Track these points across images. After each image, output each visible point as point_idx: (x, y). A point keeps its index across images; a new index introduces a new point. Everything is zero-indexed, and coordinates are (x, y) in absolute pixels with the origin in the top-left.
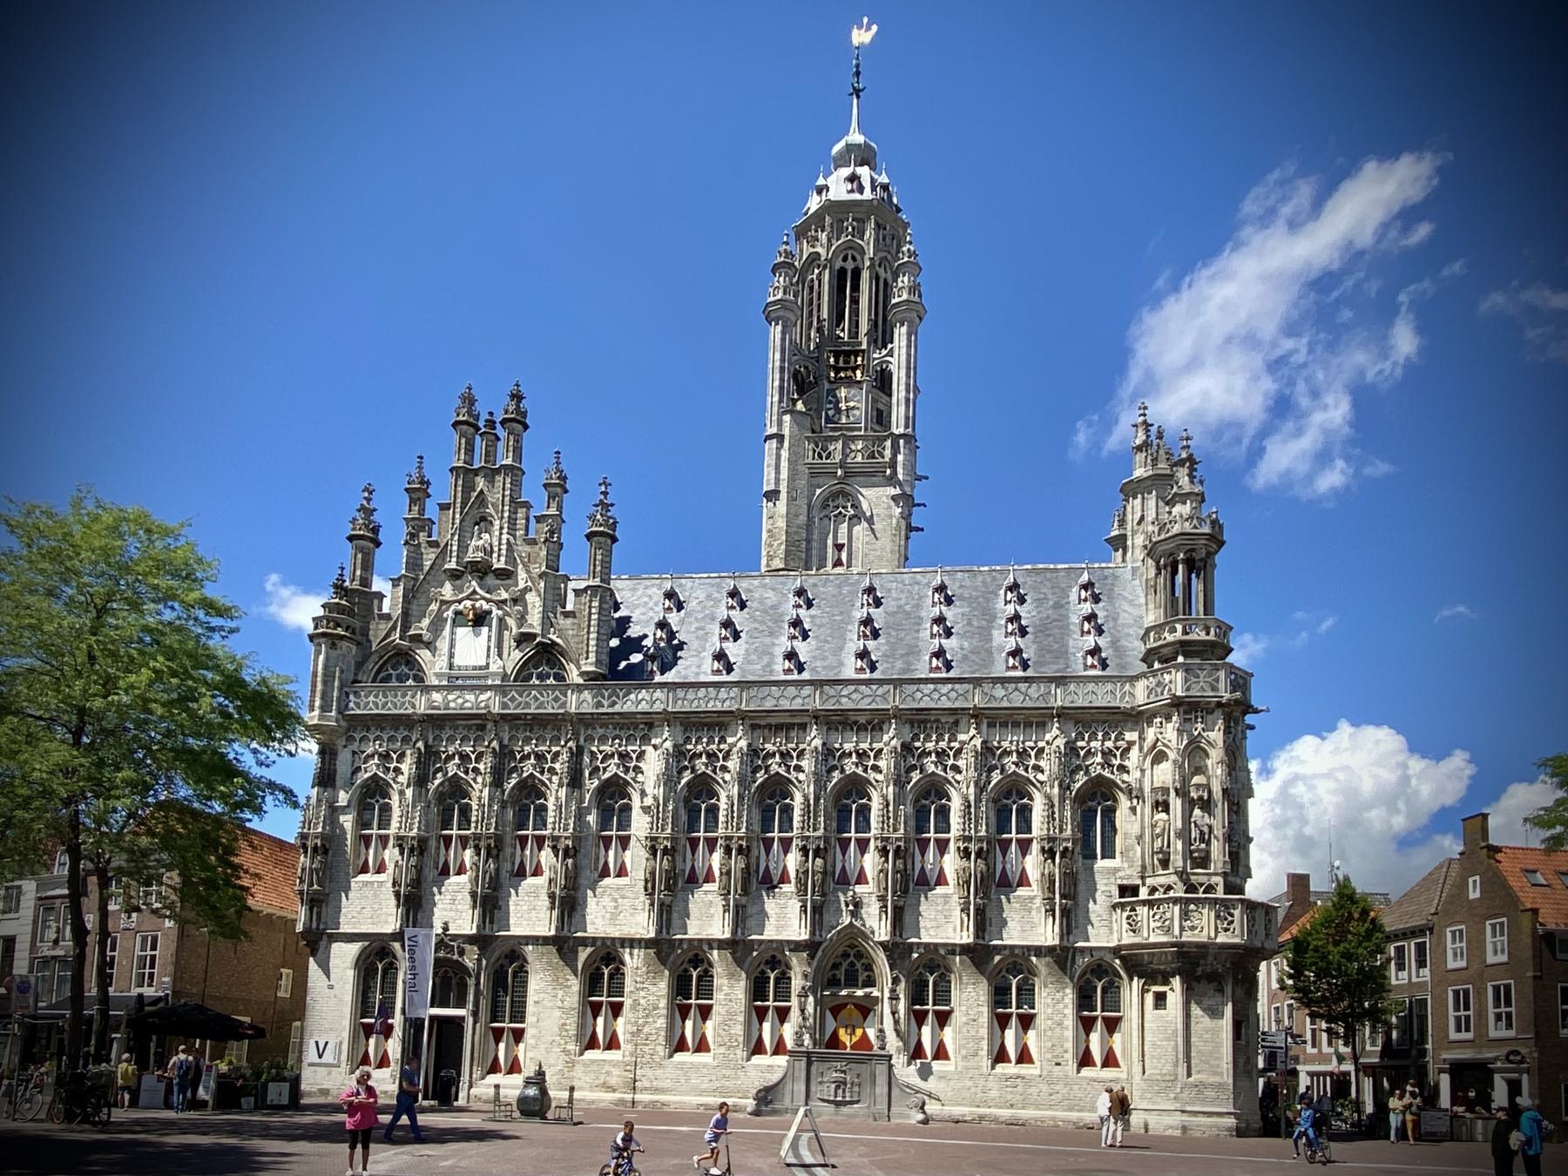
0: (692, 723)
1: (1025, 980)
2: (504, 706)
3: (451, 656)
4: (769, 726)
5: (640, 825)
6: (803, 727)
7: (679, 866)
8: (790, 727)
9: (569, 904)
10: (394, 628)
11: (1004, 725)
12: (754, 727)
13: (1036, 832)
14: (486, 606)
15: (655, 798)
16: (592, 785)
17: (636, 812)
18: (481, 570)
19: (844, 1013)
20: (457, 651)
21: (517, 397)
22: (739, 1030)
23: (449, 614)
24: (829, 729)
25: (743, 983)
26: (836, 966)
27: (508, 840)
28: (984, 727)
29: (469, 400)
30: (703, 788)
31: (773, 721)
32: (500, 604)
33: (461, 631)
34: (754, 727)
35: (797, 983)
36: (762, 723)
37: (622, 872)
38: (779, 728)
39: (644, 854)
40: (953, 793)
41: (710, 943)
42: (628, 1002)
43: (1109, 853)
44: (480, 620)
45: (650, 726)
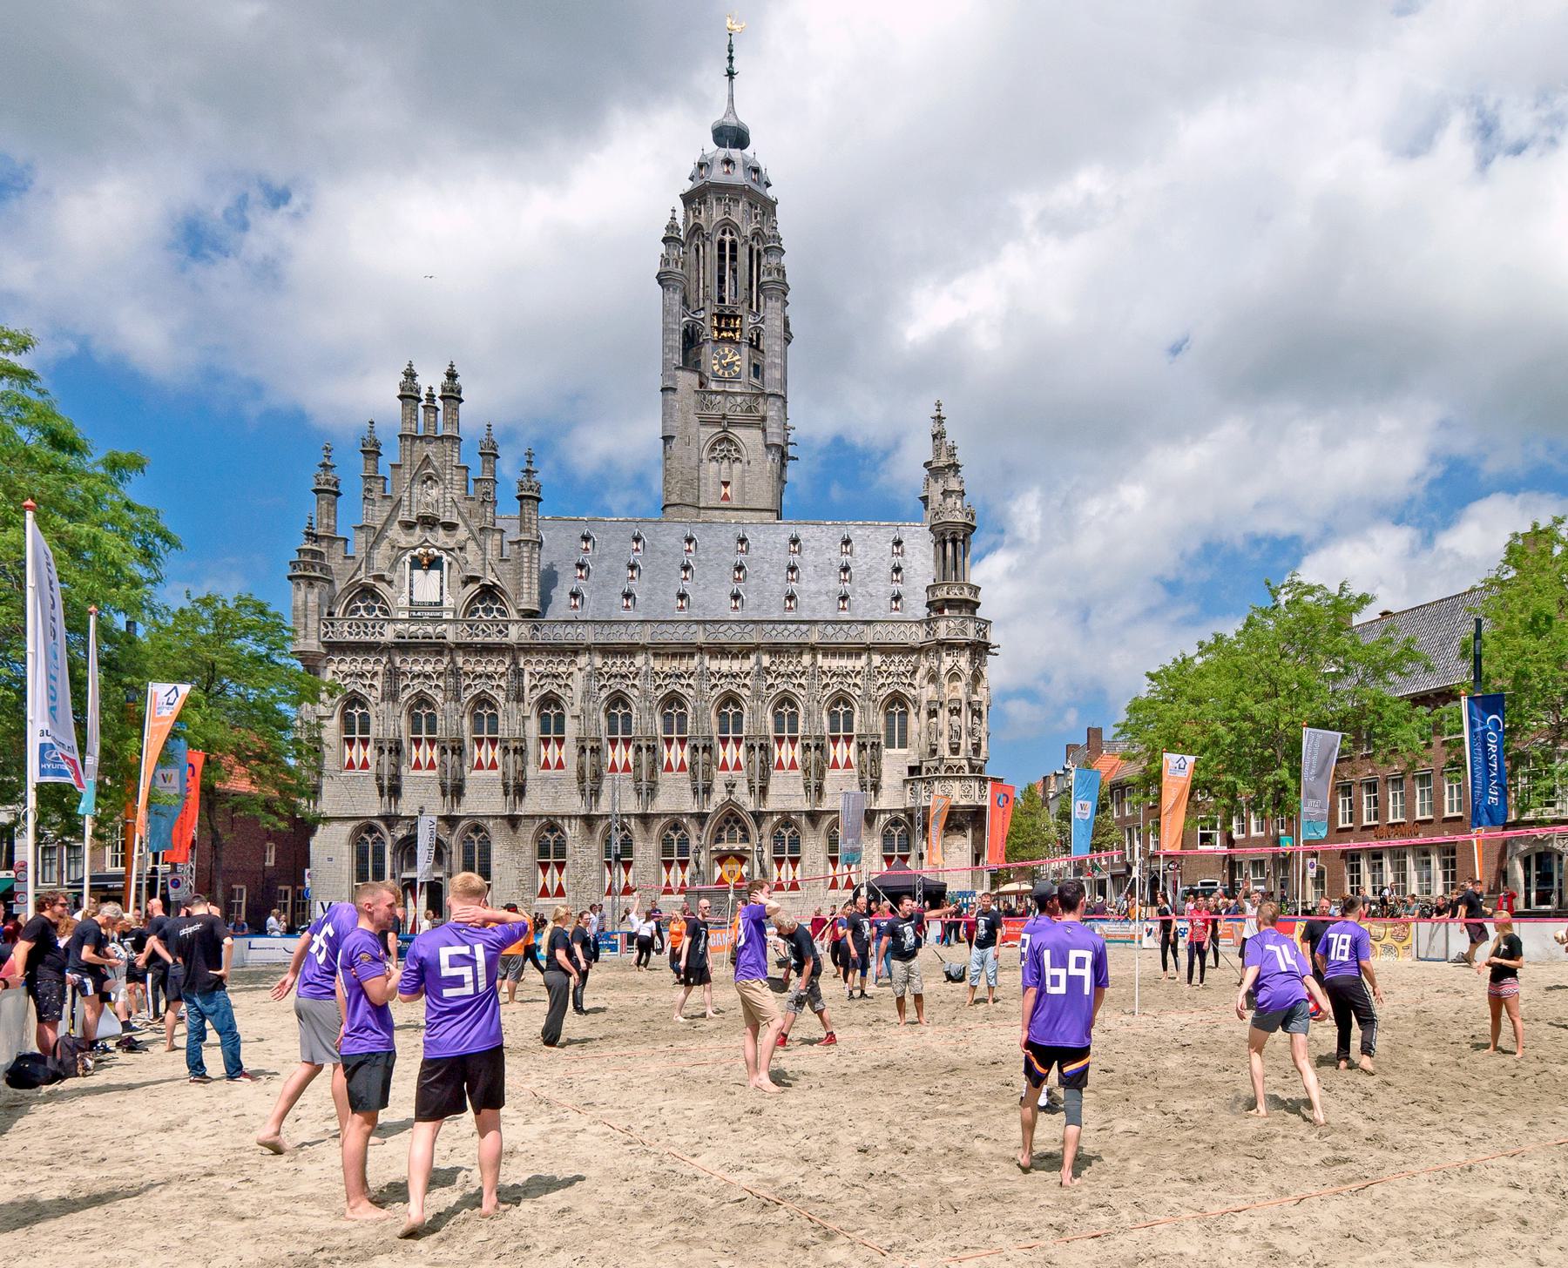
0: (607, 650)
3: (411, 593)
5: (571, 729)
8: (682, 655)
10: (359, 568)
11: (834, 655)
13: (855, 732)
14: (437, 553)
15: (582, 710)
16: (531, 697)
17: (568, 720)
18: (429, 522)
21: (452, 375)
22: (651, 878)
23: (407, 558)
26: (721, 830)
27: (467, 742)
28: (820, 657)
29: (410, 375)
30: (618, 699)
32: (448, 551)
35: (693, 843)
37: (560, 765)
38: (674, 656)
39: (576, 752)
41: (628, 816)
42: (569, 862)
43: (903, 745)
44: (435, 563)
45: (576, 653)
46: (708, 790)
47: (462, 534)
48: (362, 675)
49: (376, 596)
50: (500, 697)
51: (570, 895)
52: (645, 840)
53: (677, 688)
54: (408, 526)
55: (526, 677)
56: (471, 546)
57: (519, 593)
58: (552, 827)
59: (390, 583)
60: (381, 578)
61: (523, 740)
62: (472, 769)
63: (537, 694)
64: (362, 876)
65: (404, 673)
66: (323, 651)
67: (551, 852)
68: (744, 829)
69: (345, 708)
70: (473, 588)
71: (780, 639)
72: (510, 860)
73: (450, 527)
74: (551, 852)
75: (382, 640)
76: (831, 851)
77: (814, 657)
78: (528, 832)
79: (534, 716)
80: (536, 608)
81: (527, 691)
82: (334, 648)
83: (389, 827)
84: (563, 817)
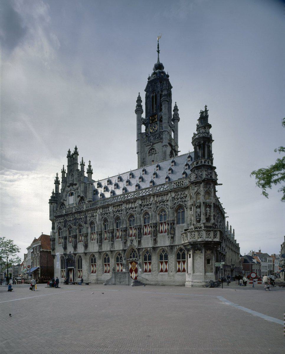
1: (166, 254)
2: (76, 210)
3: (69, 202)
4: (116, 206)
5: (96, 230)
6: (122, 205)
7: (103, 237)
8: (119, 205)
9: (86, 246)
12: (114, 206)
14: (72, 191)
19: (133, 263)
20: (70, 201)
23: (68, 194)
24: (127, 204)
25: (114, 259)
26: (131, 254)
28: (156, 198)
31: (117, 204)
33: (70, 197)
34: (114, 206)
36: (115, 205)
40: (150, 214)
41: (108, 251)
44: (72, 194)
46: (125, 243)
47: (77, 186)
48: (61, 223)
49: (64, 205)
50: (83, 224)
51: (97, 273)
52: (112, 258)
53: (118, 215)
54: (69, 187)
55: (88, 218)
56: (79, 188)
57: (86, 197)
58: (94, 256)
59: (66, 201)
60: (64, 200)
61: (87, 234)
62: (79, 242)
63: (90, 221)
64: (62, 268)
65: (67, 221)
66: (55, 218)
67: (93, 261)
68: (136, 254)
69: (59, 230)
70: (79, 198)
71: (144, 194)
72: (85, 265)
73: (76, 184)
74: (93, 261)
75: (63, 214)
76: (160, 259)
77: (154, 197)
78: (88, 257)
79: (89, 227)
80: (91, 200)
81: (88, 221)
82: (56, 217)
83: (65, 256)
84: (95, 252)
